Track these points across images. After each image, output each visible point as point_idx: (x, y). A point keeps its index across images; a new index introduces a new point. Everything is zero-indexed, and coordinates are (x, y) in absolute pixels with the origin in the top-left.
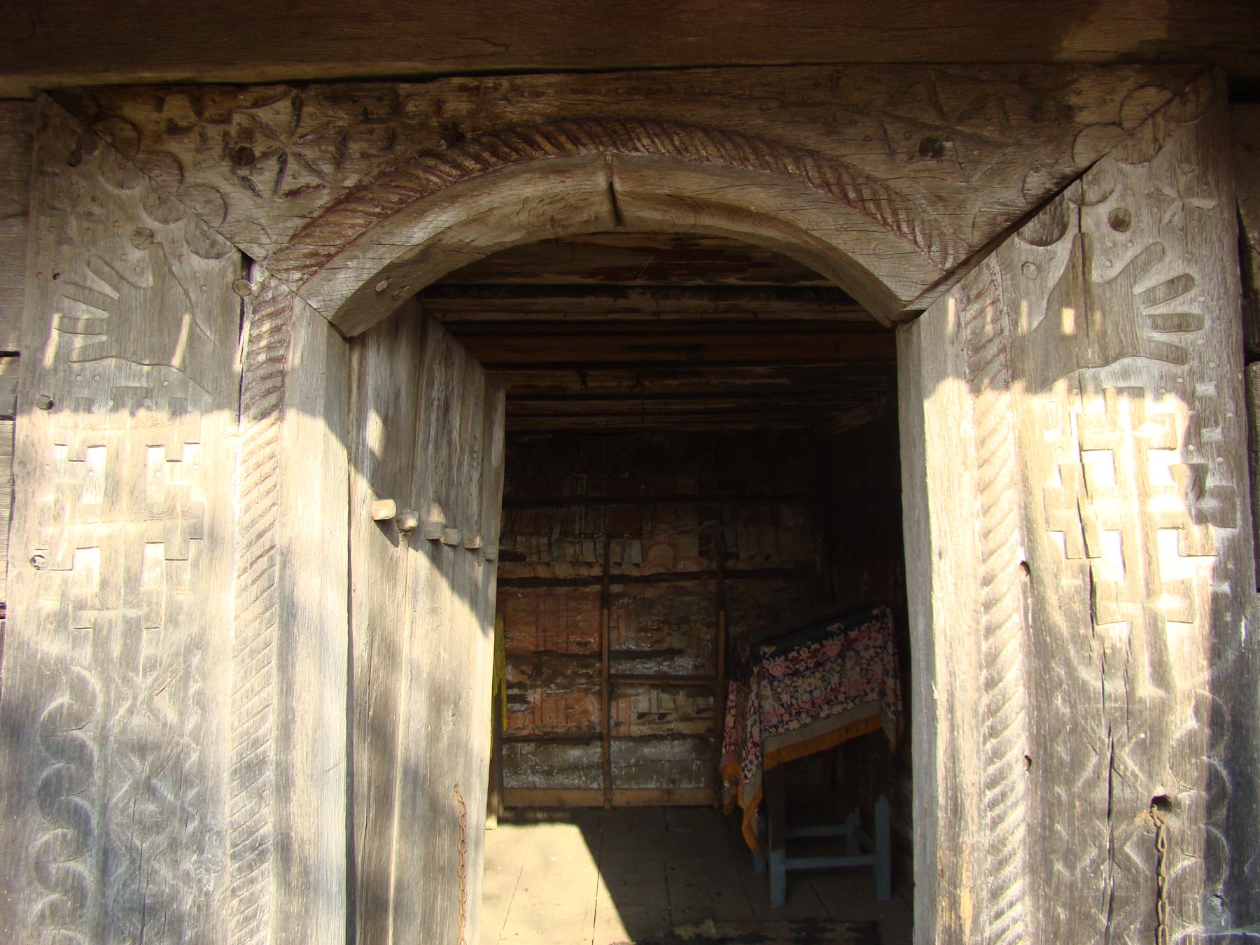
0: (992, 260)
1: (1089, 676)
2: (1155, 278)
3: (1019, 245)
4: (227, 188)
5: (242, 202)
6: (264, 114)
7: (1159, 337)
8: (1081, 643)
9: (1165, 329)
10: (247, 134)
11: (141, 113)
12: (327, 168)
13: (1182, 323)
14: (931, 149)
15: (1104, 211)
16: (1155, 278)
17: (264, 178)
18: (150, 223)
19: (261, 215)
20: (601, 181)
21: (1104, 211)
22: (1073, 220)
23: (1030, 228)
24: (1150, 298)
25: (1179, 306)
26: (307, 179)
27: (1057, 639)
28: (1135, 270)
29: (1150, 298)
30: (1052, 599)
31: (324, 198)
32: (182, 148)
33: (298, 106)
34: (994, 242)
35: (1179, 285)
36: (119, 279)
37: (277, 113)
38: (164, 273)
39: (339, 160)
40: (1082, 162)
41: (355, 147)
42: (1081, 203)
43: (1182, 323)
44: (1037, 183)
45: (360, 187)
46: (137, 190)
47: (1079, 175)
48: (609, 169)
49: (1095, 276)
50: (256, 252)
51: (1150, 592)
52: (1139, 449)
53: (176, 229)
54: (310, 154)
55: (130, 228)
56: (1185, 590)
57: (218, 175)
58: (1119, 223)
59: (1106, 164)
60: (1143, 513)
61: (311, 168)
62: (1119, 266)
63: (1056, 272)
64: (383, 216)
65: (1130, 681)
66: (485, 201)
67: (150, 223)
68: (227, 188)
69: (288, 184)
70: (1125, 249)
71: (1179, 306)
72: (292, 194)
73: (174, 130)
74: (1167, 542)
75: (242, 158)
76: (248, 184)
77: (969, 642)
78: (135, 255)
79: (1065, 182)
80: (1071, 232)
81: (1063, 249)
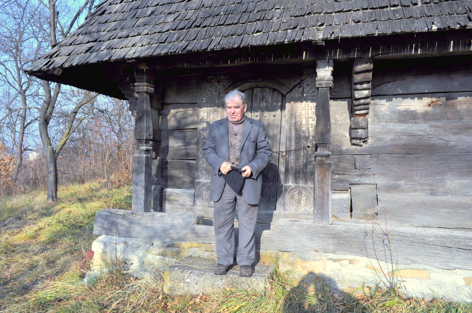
0: (293, 90)
1: (301, 133)
2: (311, 91)
3: (296, 88)
4: (217, 85)
5: (219, 86)
6: (221, 77)
7: (311, 97)
8: (300, 130)
9: (311, 97)
10: (219, 79)
11: (209, 77)
12: (227, 83)
13: (313, 96)
14: (288, 79)
15: (306, 84)
16: (311, 91)
17: (221, 84)
18: (210, 89)
19: (221, 88)
20: (254, 83)
21: (306, 84)
22: (303, 85)
23: (298, 86)
24: (310, 94)
25: (313, 94)
26: (225, 84)
27: (297, 129)
28: (309, 90)
29: (310, 94)
30: (297, 125)
31: (227, 86)
32: (213, 81)
33: (224, 76)
34: (294, 88)
35: (313, 92)
36: (207, 95)
37: (222, 77)
38: (212, 94)
39: (229, 82)
40: (304, 79)
41: (230, 81)
42: (304, 83)
43: (313, 96)
44: (298, 81)
45: (231, 85)
46: (208, 86)
47: (304, 80)
48: (255, 82)
49: (305, 91)
50: (221, 92)
51: (308, 125)
52: (308, 109)
53: (213, 90)
54: (226, 81)
55: (208, 90)
56: (312, 124)
57: (216, 84)
58: (307, 85)
59: (307, 79)
60: (308, 117)
61: (226, 83)
62: (307, 90)
63: (301, 91)
64: (233, 88)
65: (305, 134)
66: (243, 86)
67: (210, 89)
68: (217, 85)
69: (224, 85)
70: (309, 88)
71: (313, 94)
72: (224, 86)
73: (212, 79)
74: (310, 120)
75: (219, 82)
76: (219, 85)
77: (288, 130)
78: (209, 93)
79: (302, 81)
80: (302, 86)
81: (301, 89)
